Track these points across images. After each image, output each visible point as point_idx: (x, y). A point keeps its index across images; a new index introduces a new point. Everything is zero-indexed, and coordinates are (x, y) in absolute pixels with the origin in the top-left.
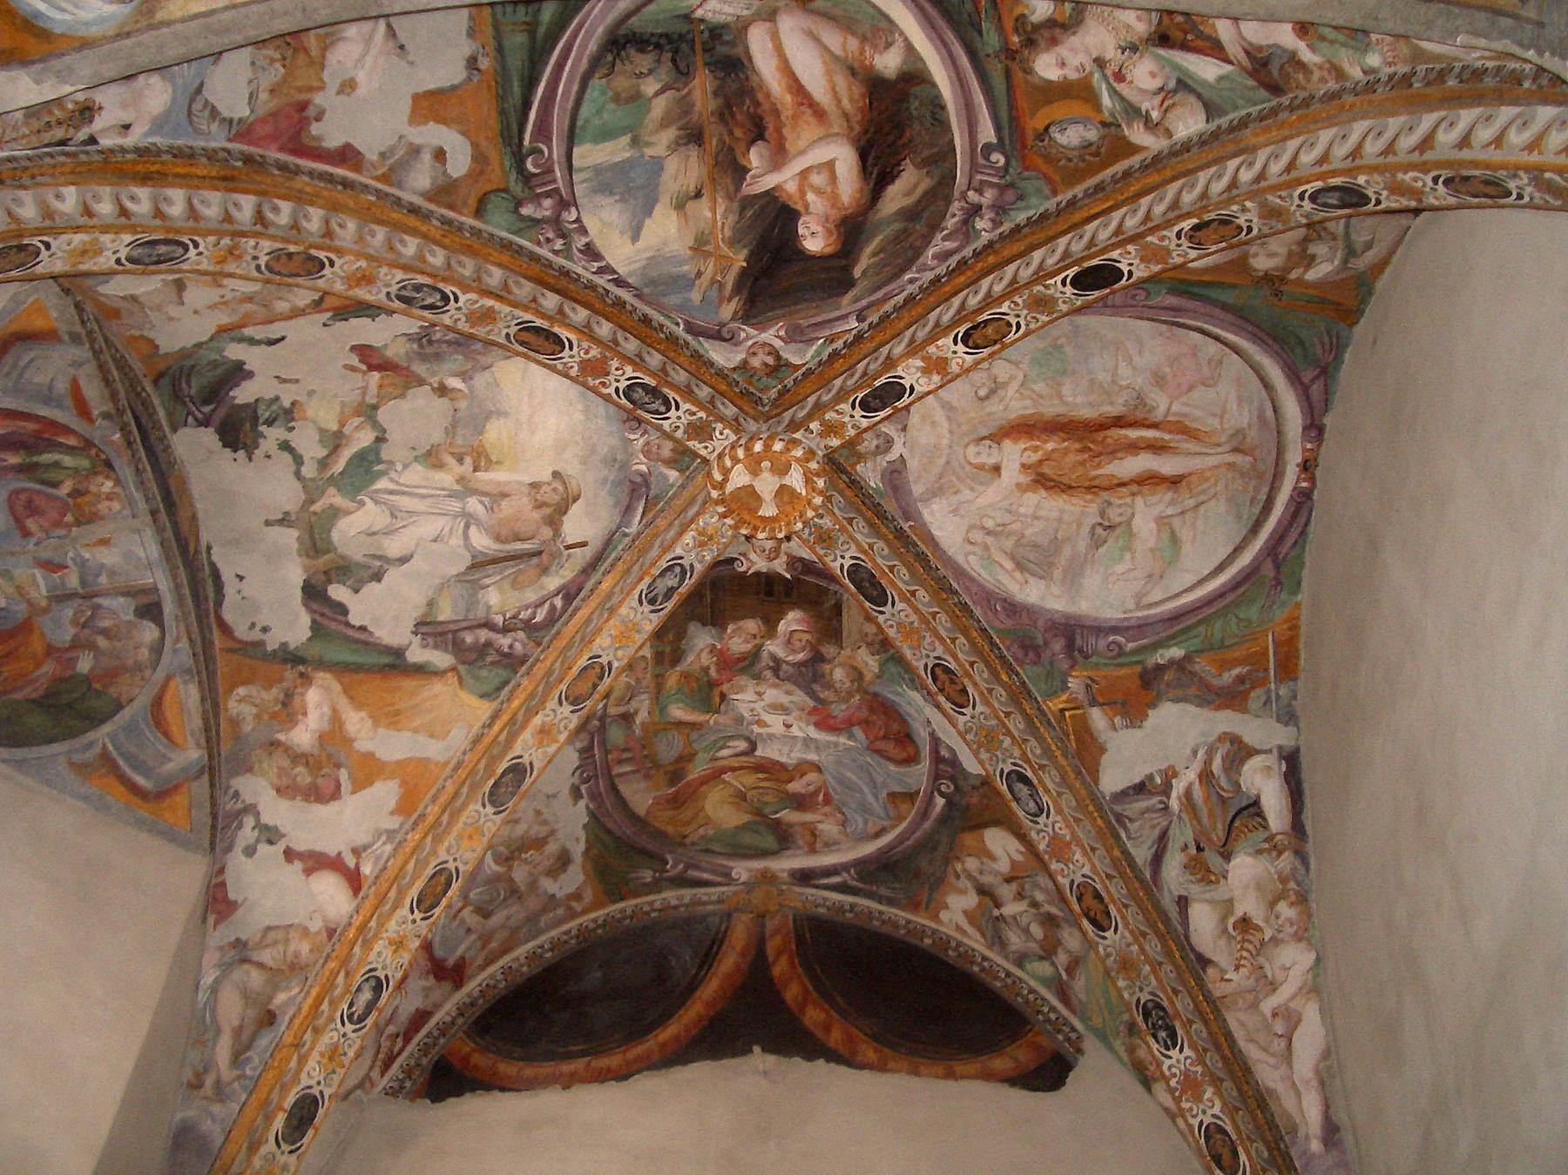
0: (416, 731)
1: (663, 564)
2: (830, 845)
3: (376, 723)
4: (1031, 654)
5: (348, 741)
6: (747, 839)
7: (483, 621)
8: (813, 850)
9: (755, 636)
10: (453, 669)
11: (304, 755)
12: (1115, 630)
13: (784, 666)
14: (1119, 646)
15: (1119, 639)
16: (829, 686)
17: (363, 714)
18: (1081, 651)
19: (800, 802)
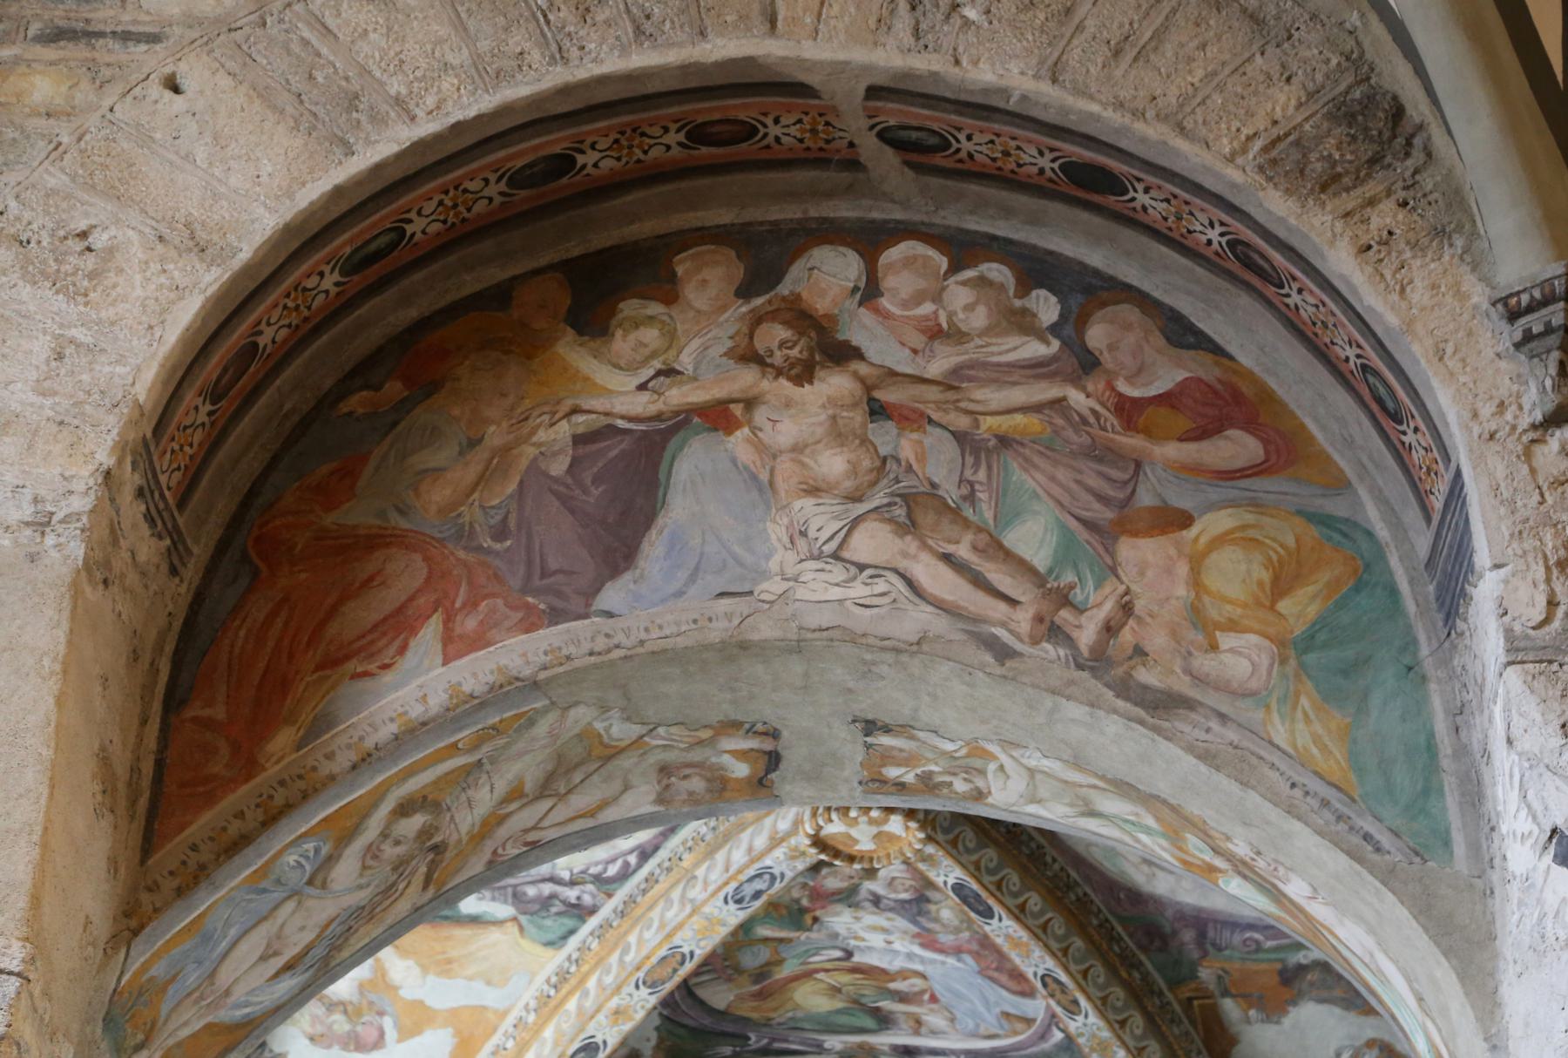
0: (470, 979)
1: (751, 872)
2: (934, 1033)
3: (425, 970)
4: (1157, 943)
5: (394, 989)
6: (844, 1020)
7: (547, 876)
8: (917, 1033)
9: (852, 877)
10: (515, 919)
11: (342, 1003)
12: (1251, 927)
13: (885, 901)
14: (1257, 942)
15: (1257, 936)
16: (937, 920)
17: (410, 963)
18: (1214, 945)
19: (903, 998)
